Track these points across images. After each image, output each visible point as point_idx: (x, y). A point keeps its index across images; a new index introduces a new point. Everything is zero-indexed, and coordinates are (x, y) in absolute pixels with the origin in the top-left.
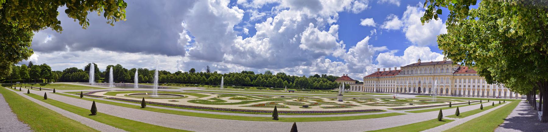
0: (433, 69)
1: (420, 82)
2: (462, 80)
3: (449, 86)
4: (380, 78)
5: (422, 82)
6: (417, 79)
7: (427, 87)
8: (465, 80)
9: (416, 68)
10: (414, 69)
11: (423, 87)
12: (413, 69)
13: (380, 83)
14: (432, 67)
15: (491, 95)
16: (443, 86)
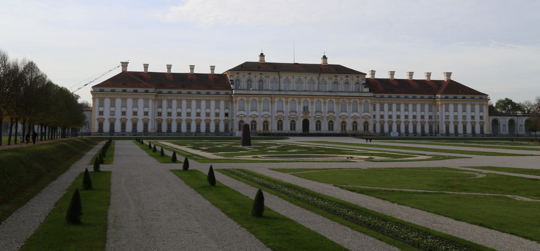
0: (317, 81)
1: (306, 109)
2: (386, 106)
3: (370, 117)
4: (161, 93)
5: (312, 109)
6: (300, 103)
7: (325, 119)
8: (398, 105)
9: (273, 75)
10: (266, 77)
11: (315, 120)
12: (263, 76)
13: (160, 106)
14: (315, 77)
15: (443, 131)
16: (358, 117)
